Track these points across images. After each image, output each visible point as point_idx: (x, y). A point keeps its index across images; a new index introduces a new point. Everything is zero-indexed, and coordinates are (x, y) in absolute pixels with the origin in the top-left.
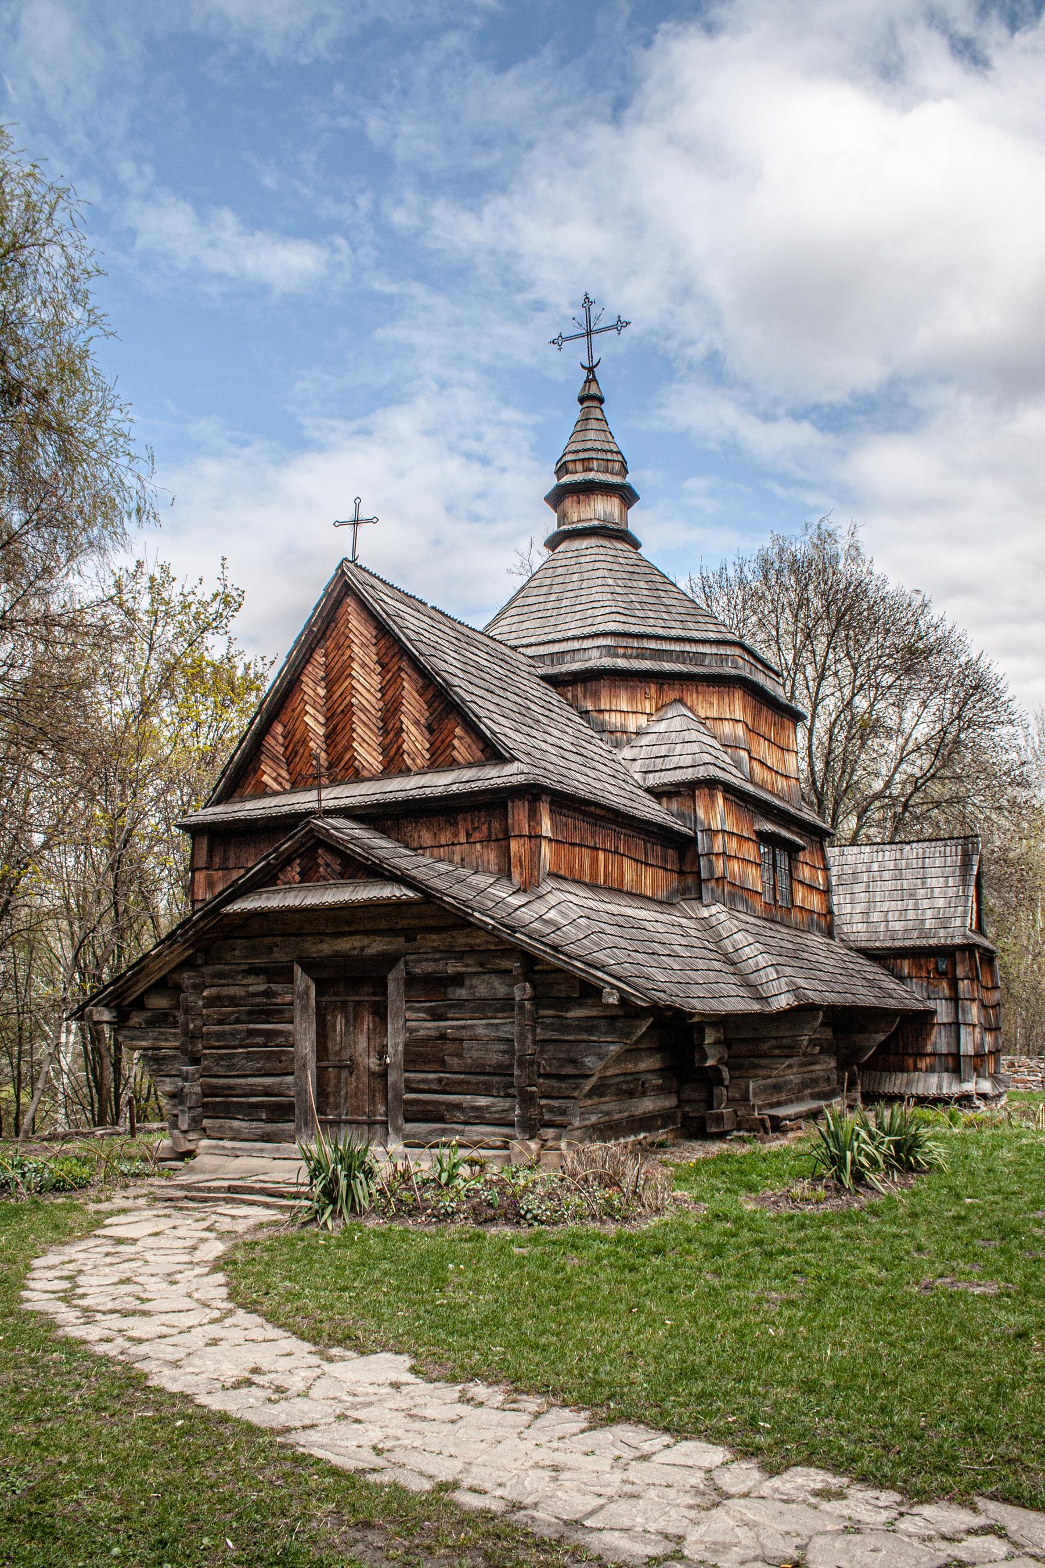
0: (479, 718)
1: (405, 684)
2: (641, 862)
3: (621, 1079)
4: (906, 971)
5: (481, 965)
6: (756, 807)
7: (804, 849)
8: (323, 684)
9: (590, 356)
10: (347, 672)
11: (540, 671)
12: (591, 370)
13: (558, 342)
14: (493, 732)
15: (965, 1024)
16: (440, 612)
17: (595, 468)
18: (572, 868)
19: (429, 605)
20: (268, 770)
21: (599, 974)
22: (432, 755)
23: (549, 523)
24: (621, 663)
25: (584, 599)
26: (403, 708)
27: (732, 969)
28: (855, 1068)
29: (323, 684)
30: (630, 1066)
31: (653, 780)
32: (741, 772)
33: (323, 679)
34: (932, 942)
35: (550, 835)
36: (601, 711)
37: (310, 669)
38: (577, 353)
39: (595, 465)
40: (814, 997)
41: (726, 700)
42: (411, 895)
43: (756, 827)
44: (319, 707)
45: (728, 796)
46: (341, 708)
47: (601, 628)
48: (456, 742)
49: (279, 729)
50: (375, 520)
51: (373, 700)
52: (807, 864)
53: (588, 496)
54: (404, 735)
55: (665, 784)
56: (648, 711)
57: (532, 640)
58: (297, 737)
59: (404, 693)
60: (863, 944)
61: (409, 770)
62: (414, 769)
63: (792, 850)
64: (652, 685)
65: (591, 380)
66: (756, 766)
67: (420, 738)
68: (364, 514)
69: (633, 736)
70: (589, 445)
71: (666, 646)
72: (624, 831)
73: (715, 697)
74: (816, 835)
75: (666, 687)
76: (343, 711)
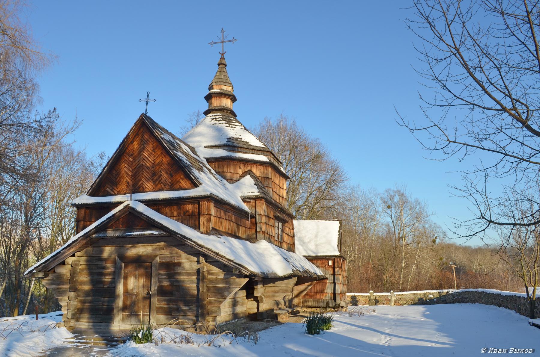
1: (163, 159)
7: (287, 222)
9: (223, 50)
10: (142, 153)
12: (223, 54)
13: (212, 43)
20: (109, 186)
23: (205, 106)
37: (127, 151)
44: (130, 165)
45: (267, 203)
46: (139, 166)
49: (114, 172)
50: (154, 100)
63: (284, 222)
64: (242, 164)
65: (222, 58)
68: (150, 98)
70: (221, 80)
75: (246, 165)
76: (139, 167)
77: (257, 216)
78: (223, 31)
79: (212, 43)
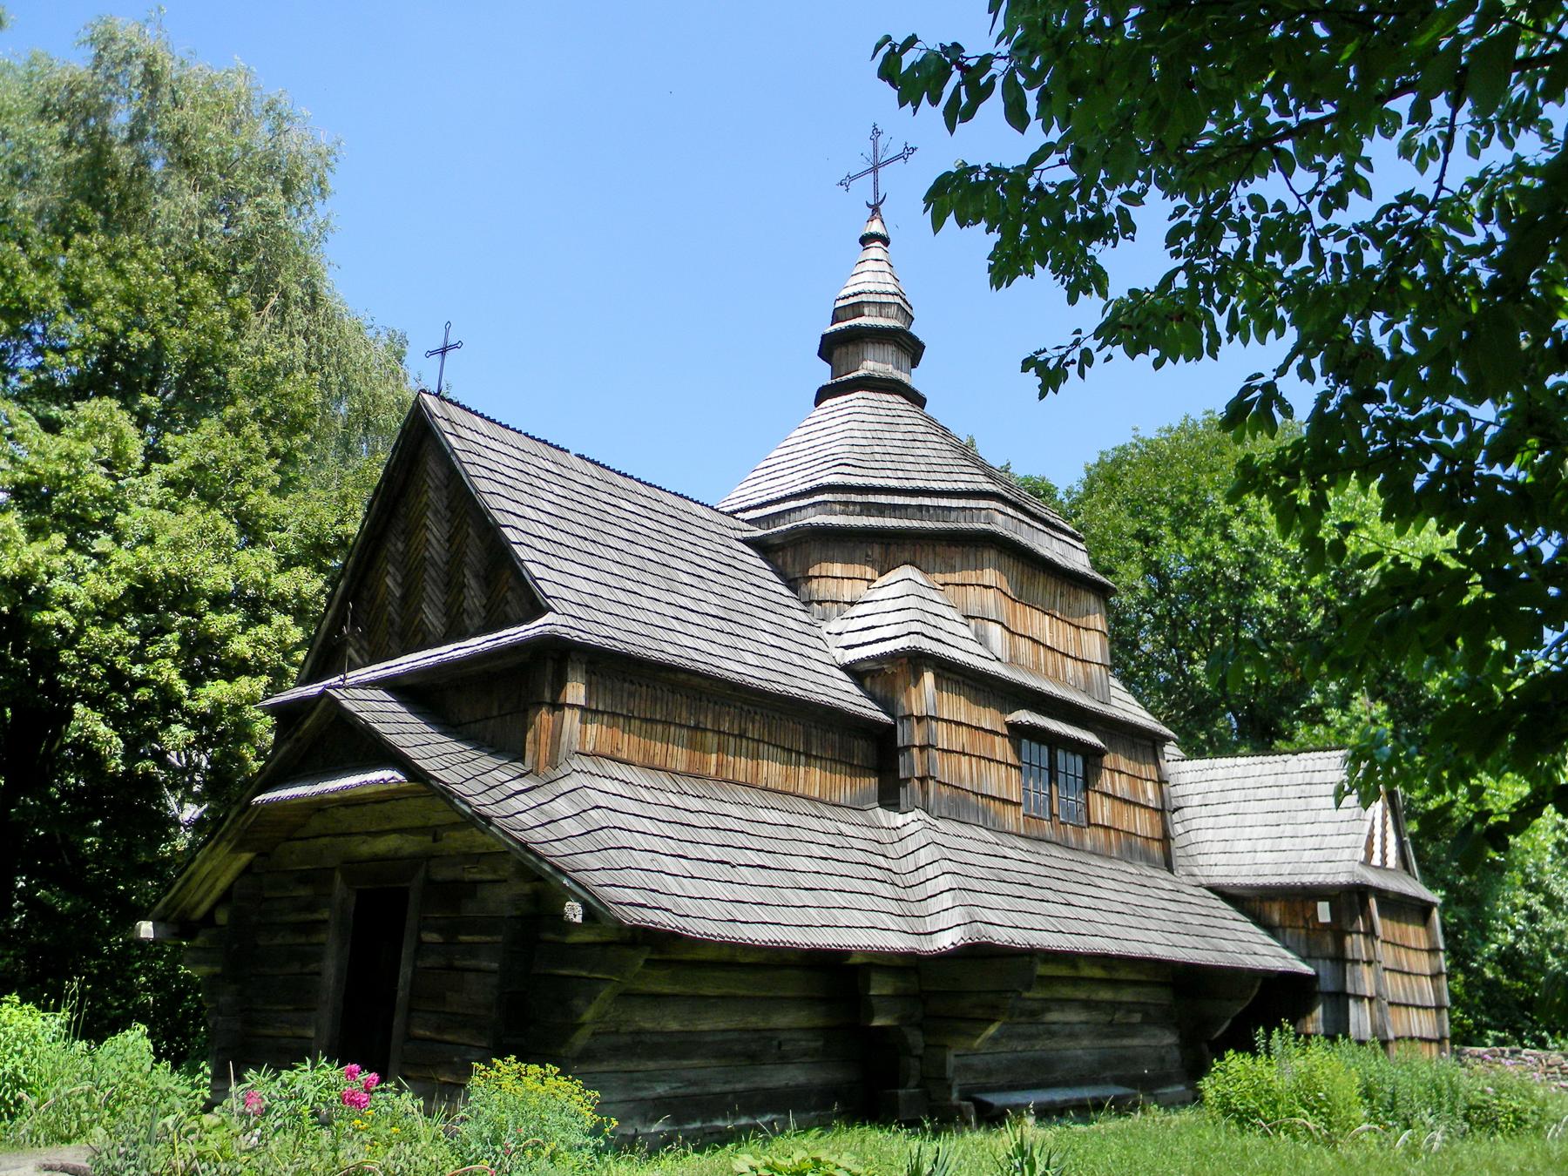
1: (470, 530)
2: (798, 753)
3: (735, 1035)
5: (495, 871)
8: (402, 538)
11: (746, 535)
13: (845, 183)
16: (592, 462)
22: (488, 612)
27: (901, 893)
28: (1205, 1047)
29: (402, 538)
30: (753, 1019)
35: (582, 702)
38: (863, 190)
40: (1001, 936)
41: (972, 558)
43: (1010, 718)
45: (947, 675)
48: (509, 595)
51: (443, 552)
52: (1120, 772)
53: (857, 345)
55: (862, 660)
56: (868, 577)
58: (378, 601)
59: (468, 541)
66: (1024, 646)
67: (479, 593)
78: (876, 132)
79: (845, 183)
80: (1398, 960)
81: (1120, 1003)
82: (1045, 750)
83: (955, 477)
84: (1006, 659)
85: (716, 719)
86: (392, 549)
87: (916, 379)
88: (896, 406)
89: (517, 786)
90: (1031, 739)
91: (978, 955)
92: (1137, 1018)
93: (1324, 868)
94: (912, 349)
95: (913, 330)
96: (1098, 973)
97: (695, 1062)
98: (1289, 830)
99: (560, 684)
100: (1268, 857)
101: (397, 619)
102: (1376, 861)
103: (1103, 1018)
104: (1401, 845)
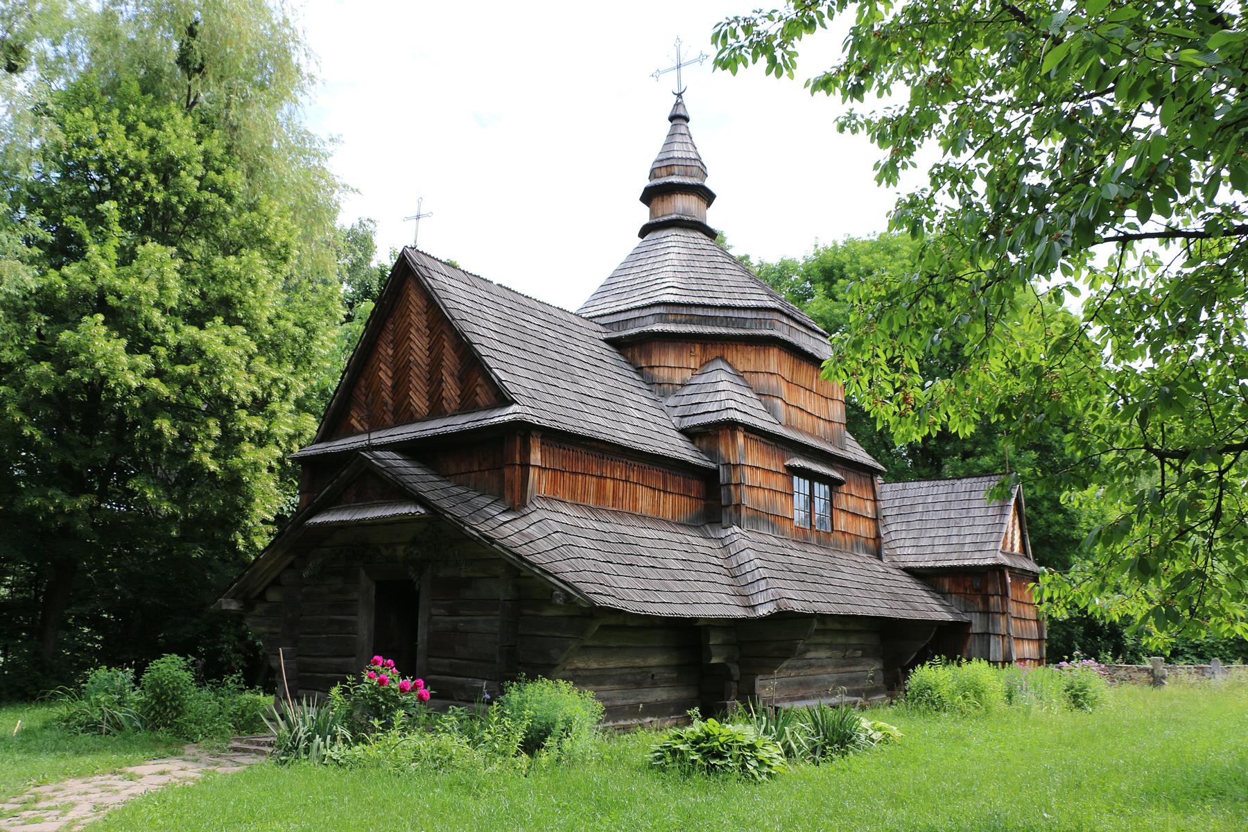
0: (490, 369)
1: (446, 344)
2: (659, 490)
3: (627, 671)
4: (947, 588)
6: (790, 447)
11: (605, 336)
12: (679, 95)
13: (656, 75)
14: (500, 380)
15: (994, 634)
16: (507, 289)
17: (676, 172)
18: (574, 492)
19: (495, 283)
20: (355, 415)
21: (551, 579)
22: (462, 400)
24: (671, 328)
25: (651, 278)
26: (443, 363)
28: (899, 670)
30: (638, 660)
31: (687, 422)
32: (774, 416)
33: (392, 342)
34: (966, 563)
36: (652, 367)
38: (669, 84)
39: (676, 169)
40: (797, 607)
42: (423, 511)
45: (751, 436)
47: (656, 300)
48: (478, 390)
49: (363, 383)
51: (424, 357)
54: (444, 384)
57: (606, 311)
59: (444, 351)
60: (910, 564)
61: (446, 412)
62: (450, 411)
66: (793, 410)
67: (454, 387)
69: (679, 388)
71: (711, 313)
72: (637, 464)
73: (753, 352)
74: (868, 472)
75: (709, 346)
77: (721, 467)
79: (656, 75)
80: (1019, 612)
81: (850, 645)
82: (807, 482)
83: (749, 297)
84: (784, 423)
85: (612, 470)
86: (384, 353)
87: (713, 217)
88: (700, 241)
89: (503, 518)
90: (800, 476)
91: (784, 619)
92: (859, 653)
93: (977, 555)
94: (707, 197)
95: (709, 184)
96: (838, 626)
97: (607, 687)
98: (955, 531)
99: (526, 453)
100: (941, 549)
101: (390, 401)
102: (1008, 550)
103: (839, 654)
104: (1022, 537)
